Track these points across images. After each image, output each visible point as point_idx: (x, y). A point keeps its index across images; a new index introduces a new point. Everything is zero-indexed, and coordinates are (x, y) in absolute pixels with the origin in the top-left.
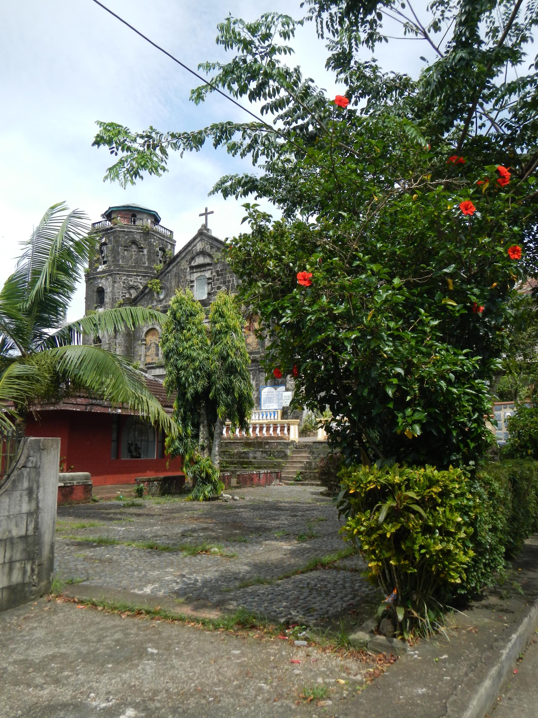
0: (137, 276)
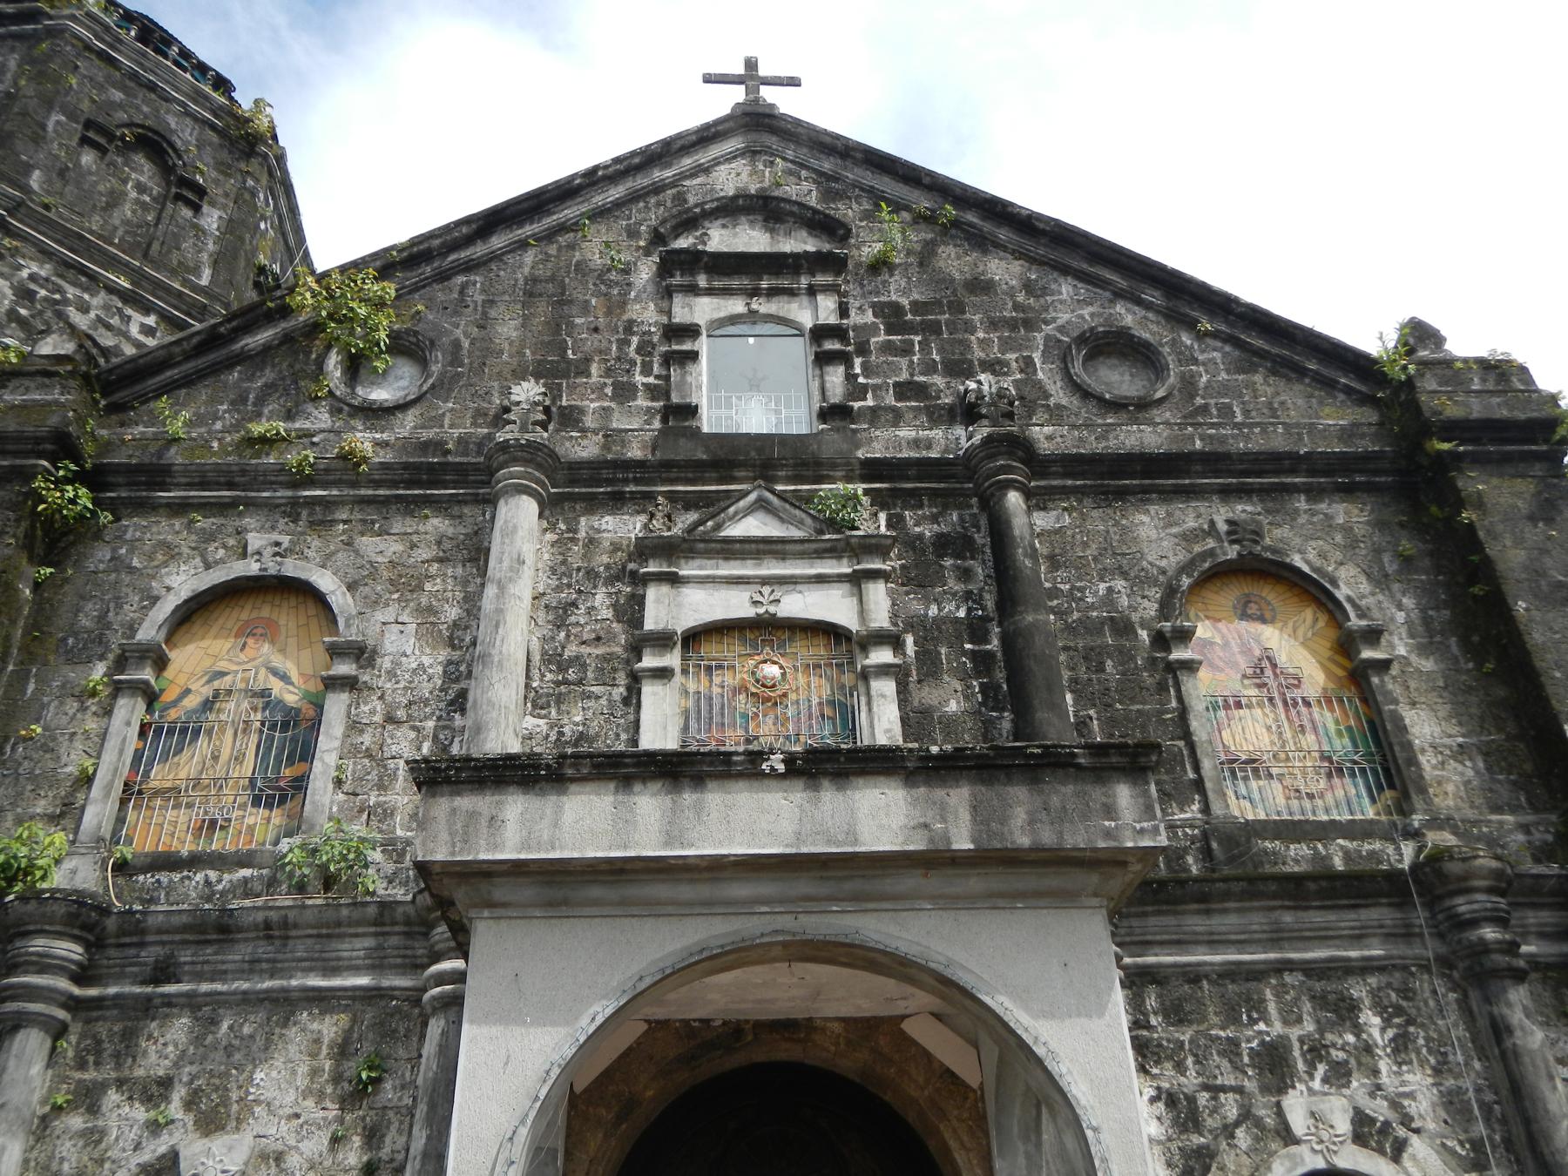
0: (128, 298)
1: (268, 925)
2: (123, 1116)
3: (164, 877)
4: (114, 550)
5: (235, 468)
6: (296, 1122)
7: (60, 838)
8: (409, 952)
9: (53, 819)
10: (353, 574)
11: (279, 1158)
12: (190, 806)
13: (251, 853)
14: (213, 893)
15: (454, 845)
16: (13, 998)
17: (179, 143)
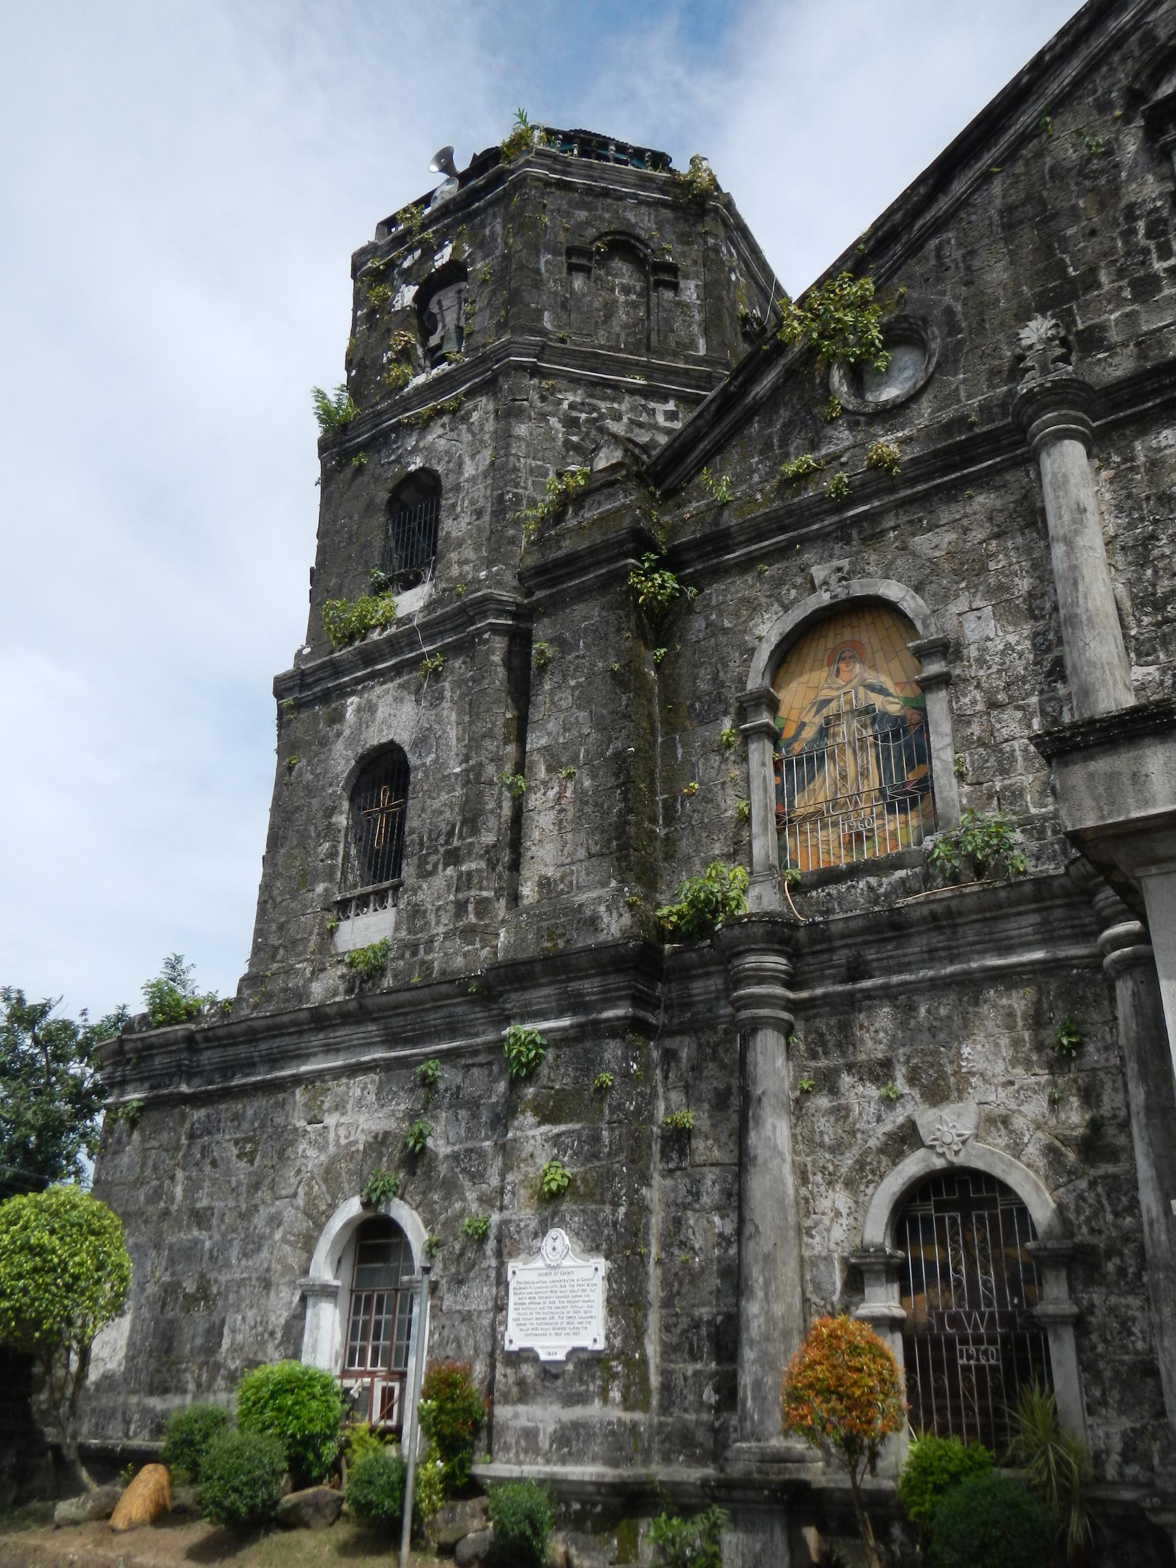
0: (649, 393)
1: (934, 917)
2: (861, 1096)
3: (832, 890)
4: (707, 618)
5: (781, 512)
6: (1011, 1089)
7: (740, 872)
8: (1076, 922)
9: (731, 857)
10: (916, 576)
11: (1005, 1121)
12: (835, 824)
13: (900, 856)
14: (878, 896)
15: (1101, 809)
16: (746, 1007)
17: (642, 234)
